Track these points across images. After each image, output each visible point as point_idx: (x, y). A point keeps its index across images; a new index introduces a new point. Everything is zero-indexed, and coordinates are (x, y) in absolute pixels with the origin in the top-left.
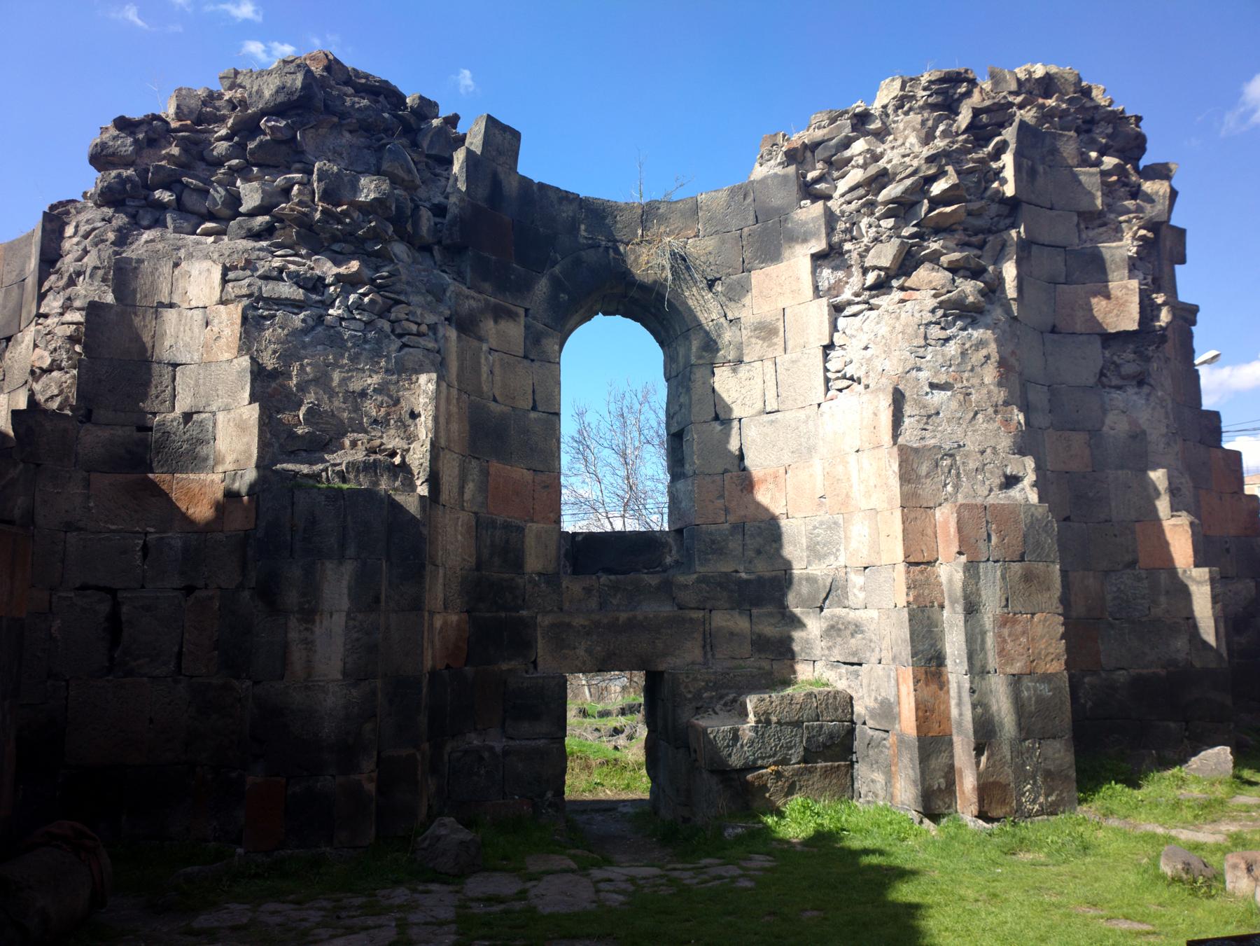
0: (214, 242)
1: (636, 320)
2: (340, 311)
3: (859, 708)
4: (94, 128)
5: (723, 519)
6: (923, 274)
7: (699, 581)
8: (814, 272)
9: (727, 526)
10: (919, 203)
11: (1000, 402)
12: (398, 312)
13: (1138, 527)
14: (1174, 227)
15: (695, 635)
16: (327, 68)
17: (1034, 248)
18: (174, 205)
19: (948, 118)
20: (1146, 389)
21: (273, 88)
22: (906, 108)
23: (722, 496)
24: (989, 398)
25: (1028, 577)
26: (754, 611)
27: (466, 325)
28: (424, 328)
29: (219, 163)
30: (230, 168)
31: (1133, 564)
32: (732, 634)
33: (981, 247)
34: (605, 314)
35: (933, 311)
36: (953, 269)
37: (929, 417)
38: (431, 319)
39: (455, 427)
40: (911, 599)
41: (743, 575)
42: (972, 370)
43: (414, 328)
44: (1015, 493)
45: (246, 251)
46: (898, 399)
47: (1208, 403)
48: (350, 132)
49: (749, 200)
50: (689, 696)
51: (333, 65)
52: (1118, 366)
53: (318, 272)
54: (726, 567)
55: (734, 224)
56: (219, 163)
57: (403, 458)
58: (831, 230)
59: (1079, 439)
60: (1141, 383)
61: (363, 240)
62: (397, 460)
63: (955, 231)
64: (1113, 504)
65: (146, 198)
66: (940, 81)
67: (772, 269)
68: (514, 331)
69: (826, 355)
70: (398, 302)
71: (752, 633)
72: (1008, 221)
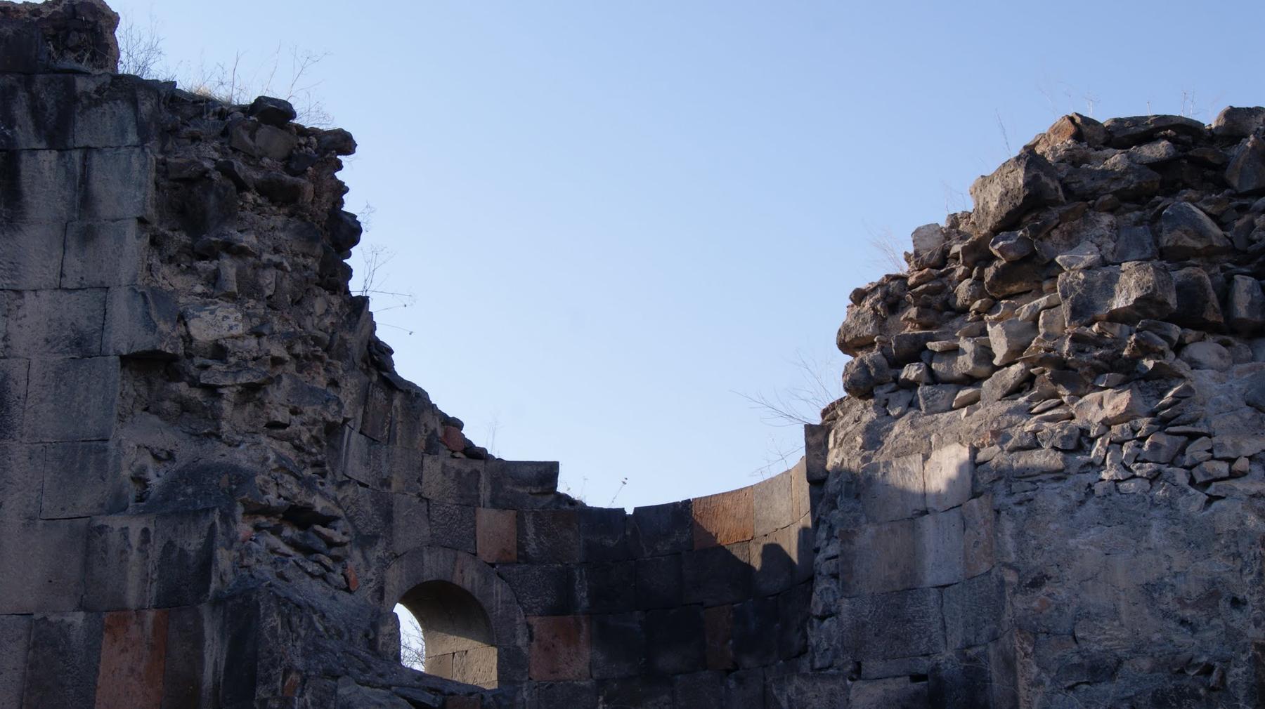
0: (968, 415)
2: (1112, 473)
4: (838, 313)
12: (1196, 450)
16: (1078, 136)
18: (925, 378)
21: (997, 196)
28: (1242, 464)
29: (965, 310)
30: (977, 312)
43: (1223, 468)
45: (995, 419)
48: (1111, 211)
51: (1083, 129)
53: (1077, 422)
56: (965, 310)
57: (1223, 677)
61: (1134, 360)
62: (1215, 677)
65: (896, 379)
70: (1193, 437)
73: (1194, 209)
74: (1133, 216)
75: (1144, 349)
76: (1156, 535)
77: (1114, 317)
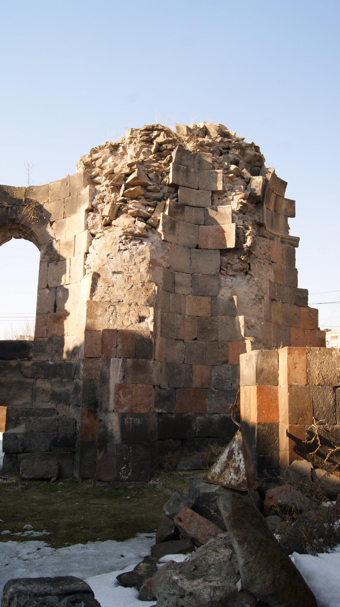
1: (31, 241)
3: (78, 428)
5: (45, 335)
7: (33, 365)
8: (86, 217)
9: (46, 339)
10: (121, 186)
11: (146, 281)
13: (229, 343)
14: (286, 200)
15: (29, 390)
17: (187, 208)
19: (148, 147)
20: (248, 277)
22: (133, 143)
23: (46, 324)
24: (141, 279)
25: (136, 367)
26: (53, 380)
31: (226, 362)
32: (43, 390)
33: (155, 206)
34: (16, 238)
35: (121, 236)
37: (109, 287)
40: (85, 375)
41: (50, 363)
42: (135, 264)
44: (143, 325)
47: (300, 286)
49: (68, 185)
50: (13, 418)
52: (232, 265)
54: (44, 359)
55: (62, 196)
58: (92, 198)
59: (205, 300)
60: (246, 273)
63: (140, 199)
64: (219, 333)
66: (146, 130)
67: (73, 217)
71: (51, 390)
72: (174, 195)
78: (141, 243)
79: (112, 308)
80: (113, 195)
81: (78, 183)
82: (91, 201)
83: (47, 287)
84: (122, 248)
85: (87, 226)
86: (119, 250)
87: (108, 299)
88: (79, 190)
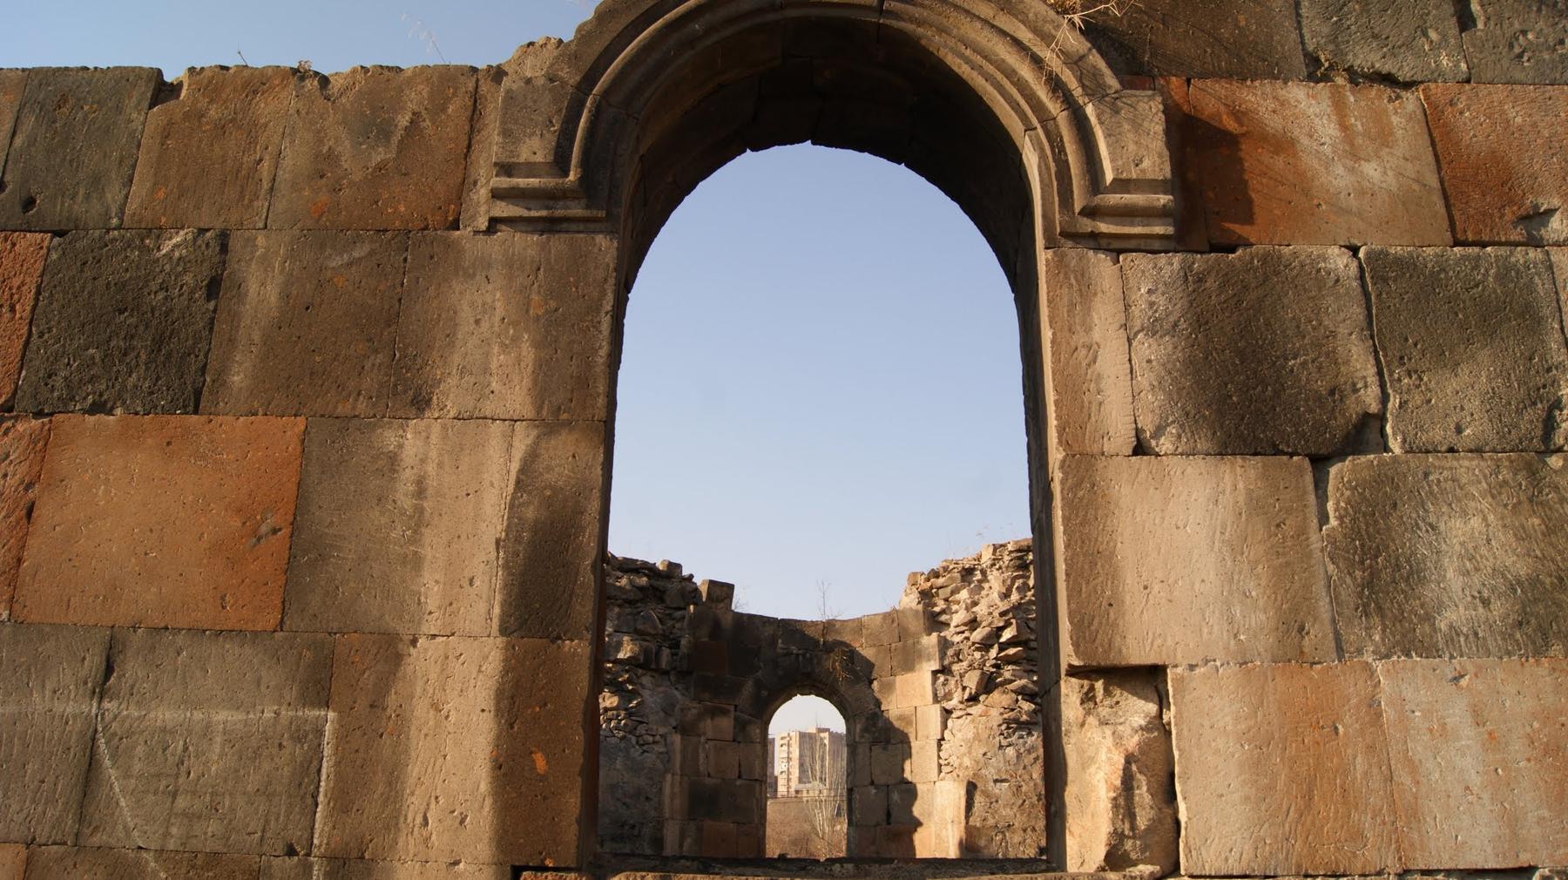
6: (996, 696)
10: (991, 646)
12: (641, 729)
23: (873, 843)
27: (685, 729)
36: (1023, 692)
38: (662, 730)
39: (677, 802)
43: (651, 739)
46: (971, 788)
58: (943, 656)
62: (636, 832)
66: (1018, 551)
67: (908, 675)
68: (726, 724)
69: (939, 745)
73: (653, 612)
74: (628, 610)
75: (629, 681)
76: (619, 764)
77: (621, 662)
78: (1030, 734)
79: (999, 837)
80: (977, 655)
81: (916, 625)
82: (942, 658)
83: (872, 783)
84: (1004, 743)
85: (936, 700)
86: (1001, 747)
87: (991, 822)
88: (917, 636)
